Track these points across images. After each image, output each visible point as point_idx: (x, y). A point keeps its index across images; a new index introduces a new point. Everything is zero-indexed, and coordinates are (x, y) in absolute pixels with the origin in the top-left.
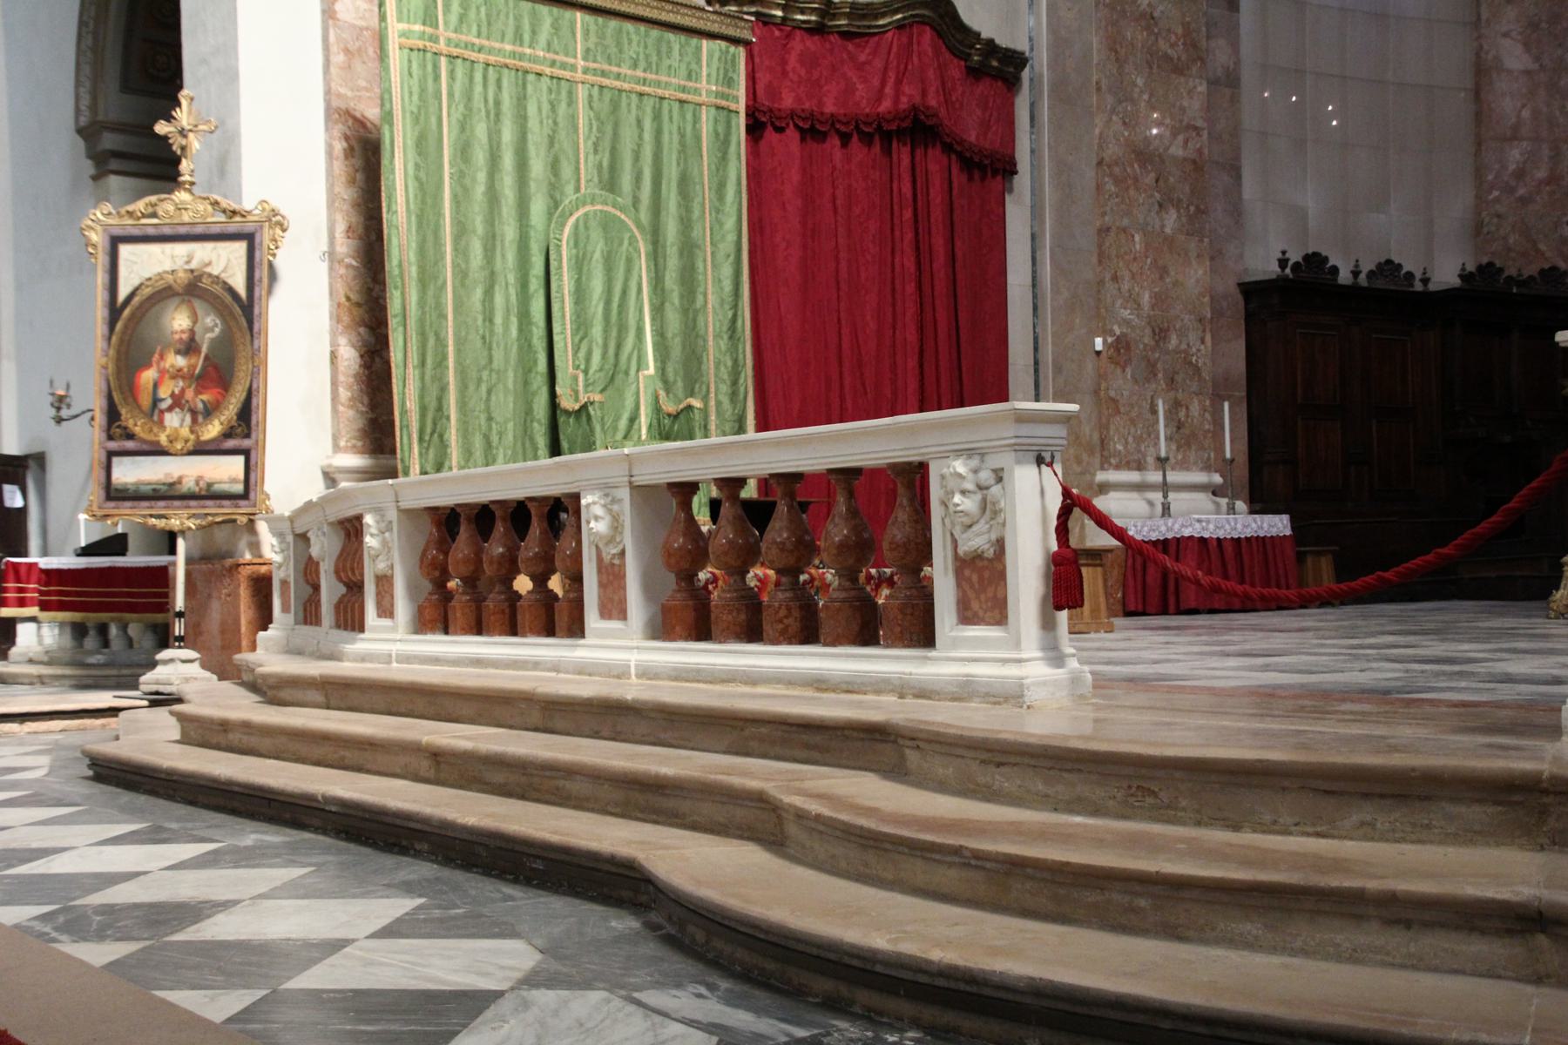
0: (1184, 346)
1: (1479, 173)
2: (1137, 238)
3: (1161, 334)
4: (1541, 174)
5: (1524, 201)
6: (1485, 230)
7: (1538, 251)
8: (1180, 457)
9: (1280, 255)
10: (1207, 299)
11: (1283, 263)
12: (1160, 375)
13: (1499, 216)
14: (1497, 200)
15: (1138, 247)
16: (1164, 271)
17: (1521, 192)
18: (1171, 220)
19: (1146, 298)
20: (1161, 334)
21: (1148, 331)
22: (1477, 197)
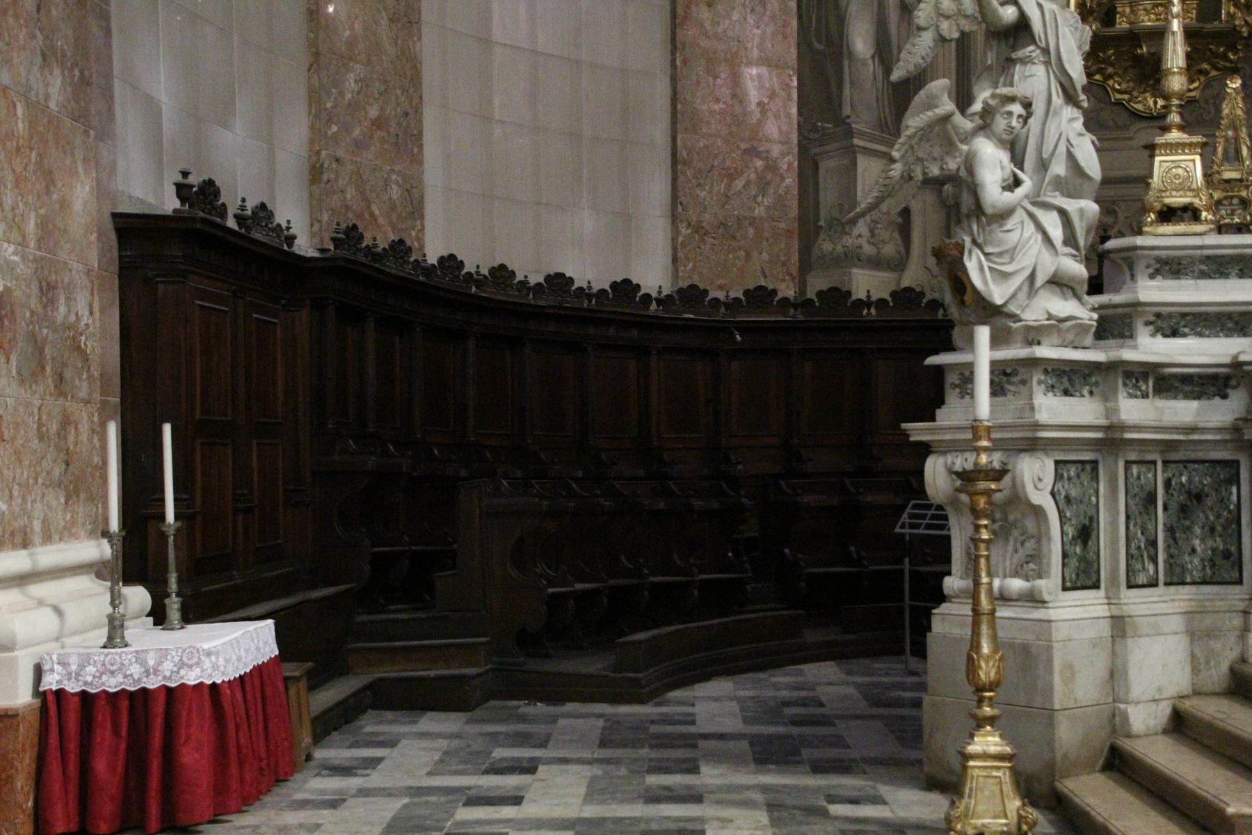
0: (72, 318)
1: (314, 96)
2: (20, 111)
3: (48, 291)
4: (373, 113)
5: (360, 145)
6: (325, 177)
7: (372, 215)
8: (68, 516)
9: (179, 178)
10: (93, 237)
11: (182, 190)
12: (48, 369)
13: (337, 160)
14: (335, 138)
15: (21, 126)
16: (49, 177)
17: (357, 132)
18: (55, 89)
19: (31, 227)
20: (48, 291)
21: (35, 287)
22: (312, 127)
